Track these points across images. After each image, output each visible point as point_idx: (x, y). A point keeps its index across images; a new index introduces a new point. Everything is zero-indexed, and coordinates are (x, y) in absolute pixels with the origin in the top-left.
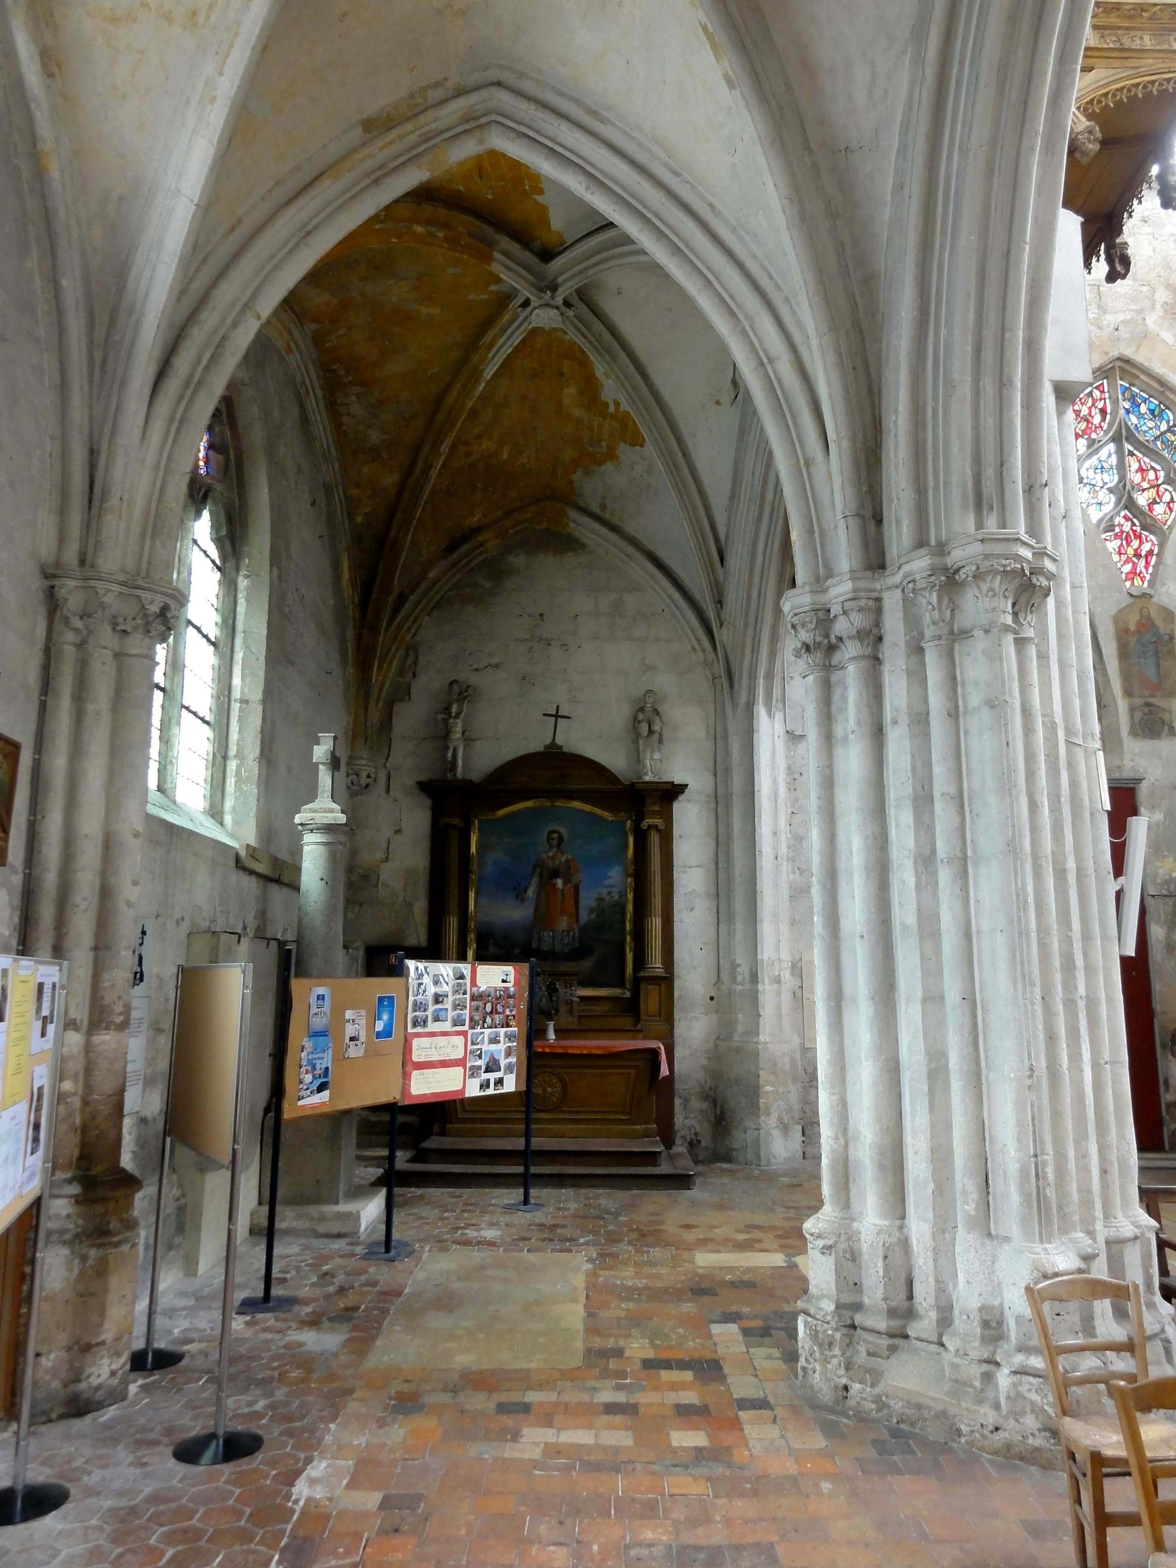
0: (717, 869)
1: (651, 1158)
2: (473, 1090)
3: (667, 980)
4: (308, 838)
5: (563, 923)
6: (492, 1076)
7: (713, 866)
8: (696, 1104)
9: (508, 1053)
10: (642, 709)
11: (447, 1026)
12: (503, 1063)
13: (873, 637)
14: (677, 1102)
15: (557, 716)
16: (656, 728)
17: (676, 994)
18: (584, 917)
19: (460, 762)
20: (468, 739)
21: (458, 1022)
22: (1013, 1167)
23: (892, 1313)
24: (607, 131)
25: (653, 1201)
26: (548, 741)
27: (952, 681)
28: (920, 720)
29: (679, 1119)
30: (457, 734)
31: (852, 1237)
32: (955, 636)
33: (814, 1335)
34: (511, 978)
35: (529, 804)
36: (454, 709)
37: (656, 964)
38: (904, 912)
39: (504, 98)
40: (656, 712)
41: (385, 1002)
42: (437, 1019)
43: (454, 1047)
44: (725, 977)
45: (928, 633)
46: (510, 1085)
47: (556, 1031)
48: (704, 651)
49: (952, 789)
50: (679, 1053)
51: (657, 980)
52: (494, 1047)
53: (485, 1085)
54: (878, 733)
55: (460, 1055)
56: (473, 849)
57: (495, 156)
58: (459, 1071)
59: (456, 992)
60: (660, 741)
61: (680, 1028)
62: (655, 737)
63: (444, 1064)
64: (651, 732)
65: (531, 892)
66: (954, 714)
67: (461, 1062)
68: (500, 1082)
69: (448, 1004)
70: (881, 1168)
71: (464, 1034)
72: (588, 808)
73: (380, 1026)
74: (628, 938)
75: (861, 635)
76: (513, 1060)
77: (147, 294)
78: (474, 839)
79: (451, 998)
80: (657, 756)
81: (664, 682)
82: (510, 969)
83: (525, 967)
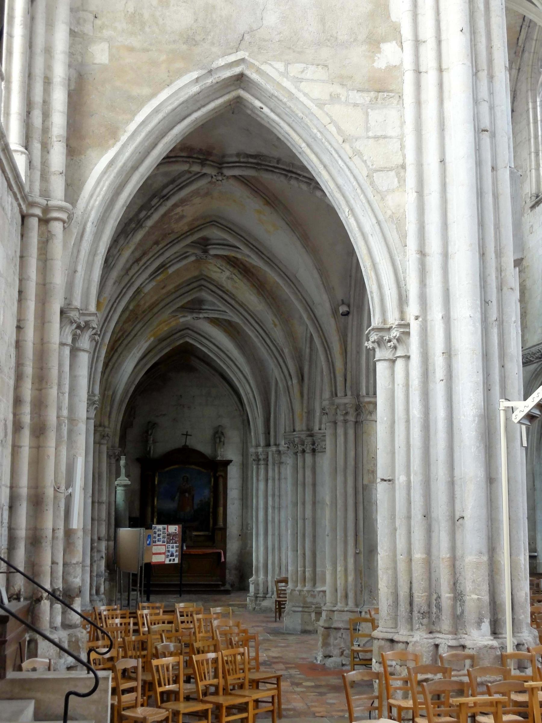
0: (243, 490)
1: (218, 586)
2: (167, 562)
3: (224, 529)
4: (118, 488)
5: (188, 509)
6: (172, 558)
7: (241, 489)
8: (233, 572)
9: (176, 551)
10: (216, 433)
11: (161, 543)
12: (175, 554)
13: (266, 460)
14: (227, 571)
15: (187, 435)
16: (222, 440)
17: (228, 534)
18: (195, 507)
19: (152, 452)
20: (154, 442)
21: (164, 542)
22: (284, 564)
23: (264, 594)
24: (213, 340)
25: (217, 597)
26: (184, 444)
27: (280, 473)
28: (274, 479)
29: (228, 577)
30: (151, 442)
31: (258, 581)
32: (281, 463)
33: (251, 600)
34: (177, 529)
35: (176, 466)
36: (150, 432)
37: (221, 524)
38: (270, 518)
39: (190, 332)
40: (222, 433)
41: (149, 536)
42: (158, 541)
43: (163, 549)
44: (244, 528)
45: (276, 462)
46: (177, 561)
47: (186, 547)
48: (240, 410)
49: (278, 494)
50: (227, 555)
51: (220, 529)
52: (172, 549)
53: (170, 560)
54: (267, 480)
55: (164, 551)
56: (156, 483)
57: (187, 343)
58: (163, 556)
59: (163, 533)
60: (224, 444)
61: (229, 546)
62: (222, 443)
63: (160, 554)
64: (220, 441)
65: (177, 498)
66: (279, 479)
67: (164, 553)
68: (174, 560)
69: (161, 537)
70: (263, 567)
71: (165, 545)
72: (197, 468)
73: (148, 542)
74: (211, 514)
75: (264, 460)
76: (177, 553)
77: (118, 390)
78: (156, 479)
79: (162, 535)
80: (222, 450)
81: (225, 422)
82: (177, 526)
83: (181, 526)
